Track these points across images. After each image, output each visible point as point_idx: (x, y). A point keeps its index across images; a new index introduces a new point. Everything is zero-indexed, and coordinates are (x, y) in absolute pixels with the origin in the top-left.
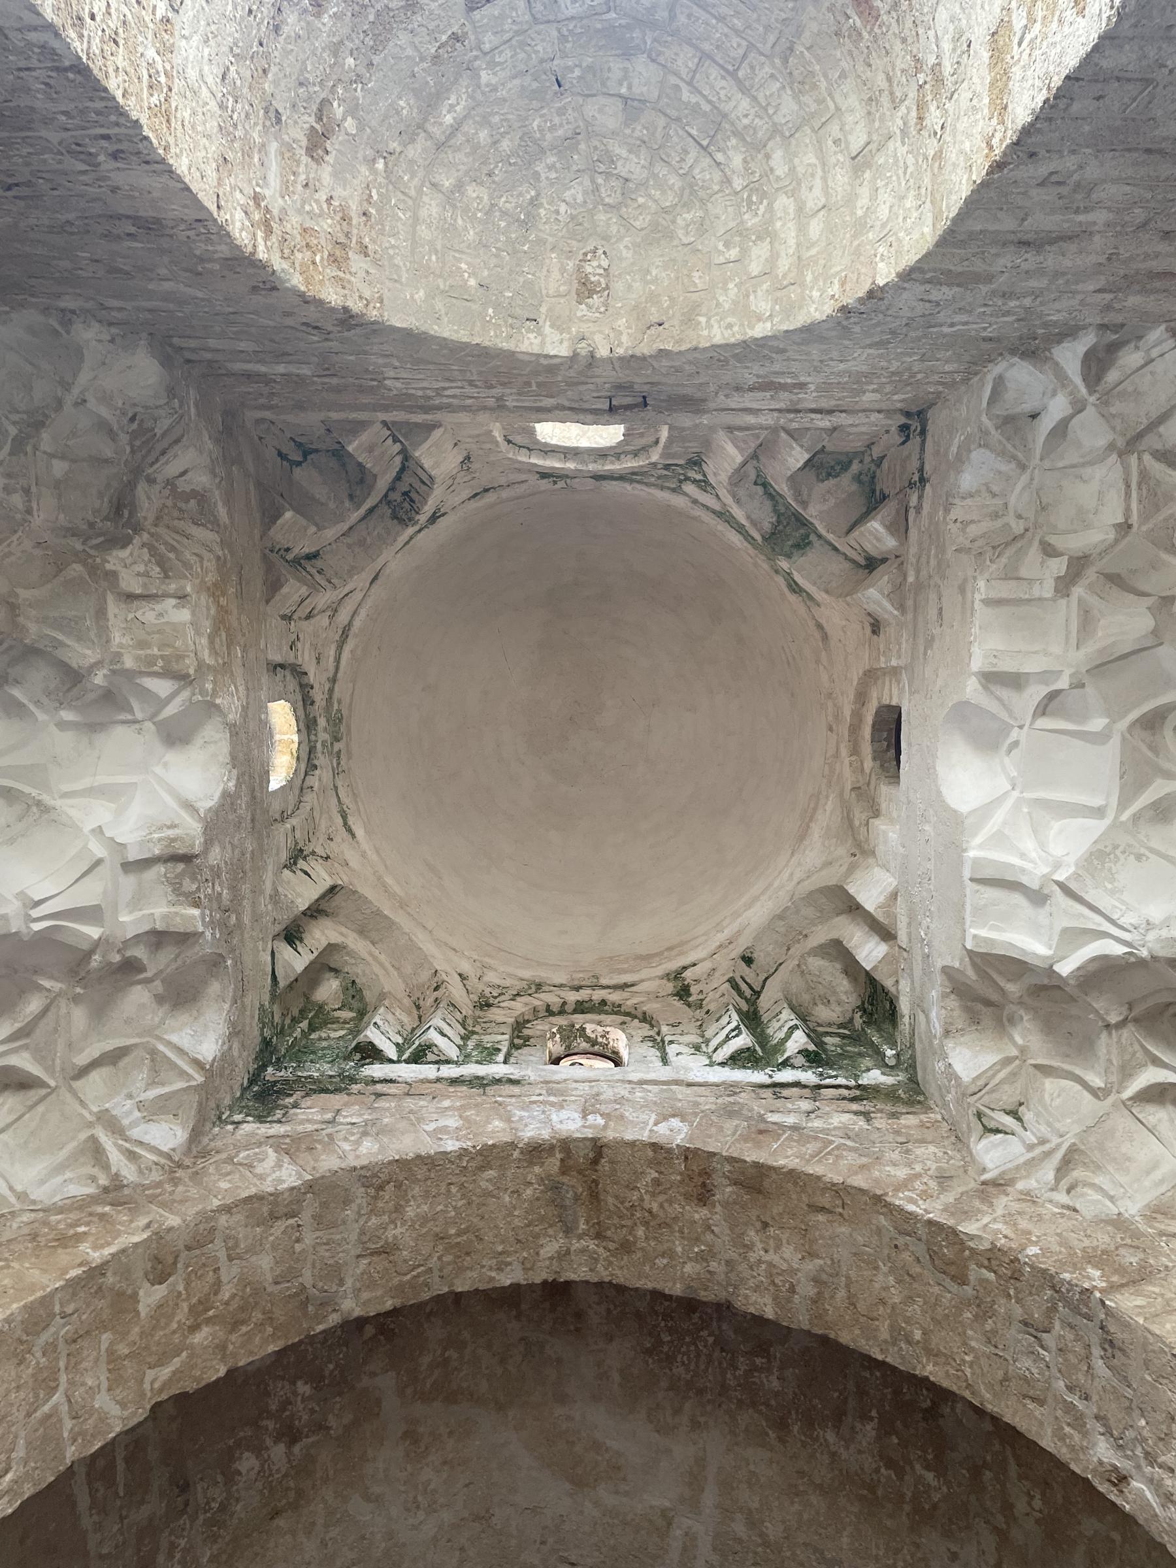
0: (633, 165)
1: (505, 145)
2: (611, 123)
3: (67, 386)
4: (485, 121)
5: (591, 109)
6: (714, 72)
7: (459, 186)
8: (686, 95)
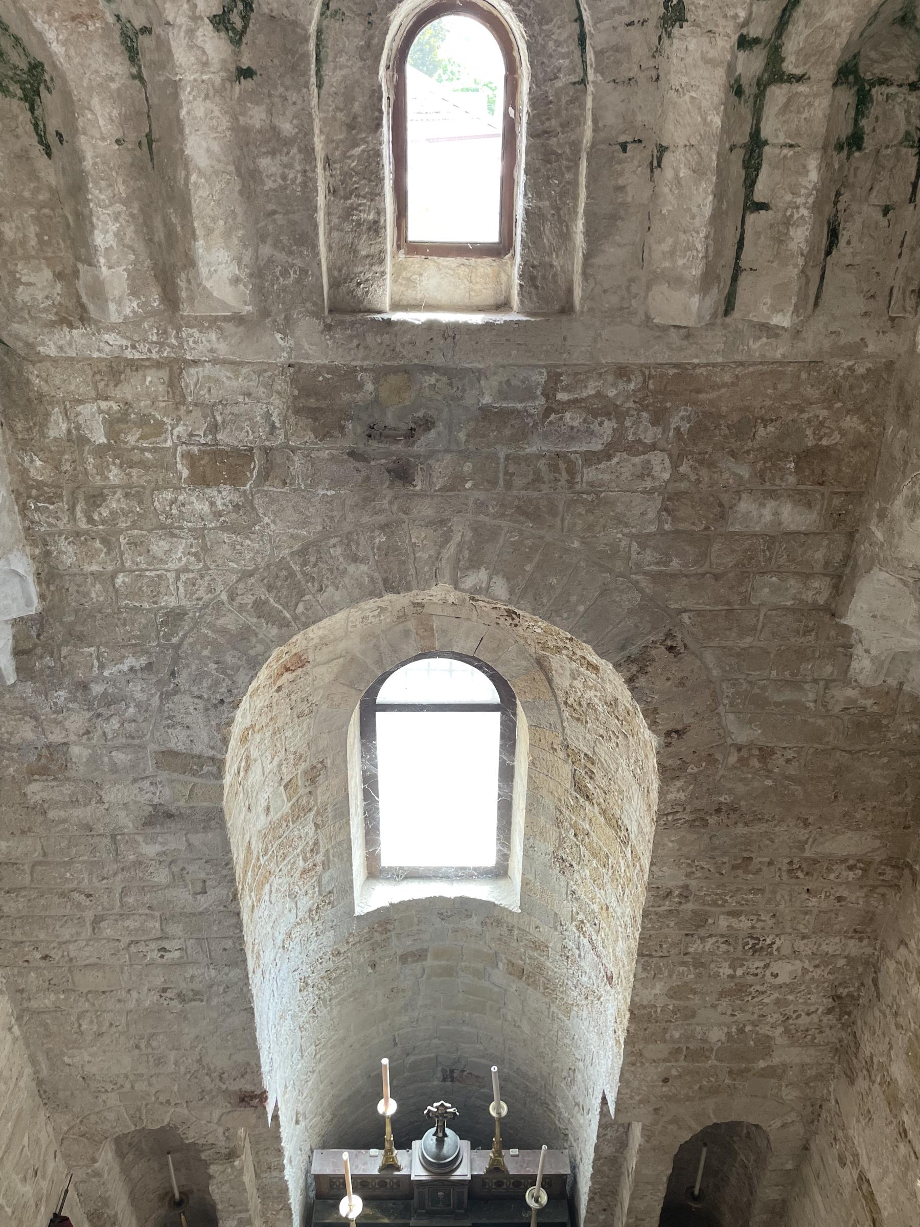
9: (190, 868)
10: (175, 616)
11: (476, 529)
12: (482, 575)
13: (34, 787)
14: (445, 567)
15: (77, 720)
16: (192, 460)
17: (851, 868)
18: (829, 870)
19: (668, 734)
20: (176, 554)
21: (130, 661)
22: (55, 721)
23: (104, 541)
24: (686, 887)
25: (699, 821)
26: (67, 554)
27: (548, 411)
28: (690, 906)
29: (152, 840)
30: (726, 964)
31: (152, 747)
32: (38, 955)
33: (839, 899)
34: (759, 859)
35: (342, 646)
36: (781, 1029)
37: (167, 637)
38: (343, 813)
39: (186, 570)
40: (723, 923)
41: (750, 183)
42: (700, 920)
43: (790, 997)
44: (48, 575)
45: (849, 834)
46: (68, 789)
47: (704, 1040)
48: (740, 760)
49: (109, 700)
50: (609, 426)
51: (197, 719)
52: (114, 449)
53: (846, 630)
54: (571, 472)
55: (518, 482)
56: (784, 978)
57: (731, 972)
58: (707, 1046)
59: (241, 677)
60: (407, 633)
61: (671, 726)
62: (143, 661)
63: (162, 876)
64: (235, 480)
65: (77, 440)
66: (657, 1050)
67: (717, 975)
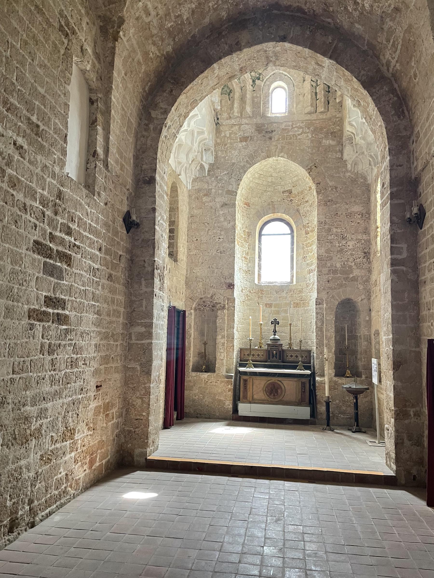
0: (270, 170)
1: (288, 173)
2: (273, 174)
3: (357, 157)
4: (291, 176)
5: (277, 175)
6: (261, 183)
7: (295, 171)
8: (264, 179)
9: (228, 217)
10: (234, 164)
11: (282, 146)
12: (283, 154)
13: (205, 198)
14: (277, 153)
15: (214, 184)
16: (240, 138)
17: (359, 215)
18: (355, 215)
19: (317, 184)
20: (235, 153)
21: (225, 172)
22: (211, 184)
23: (226, 152)
24: (325, 220)
25: (326, 204)
26: (220, 153)
27: (292, 128)
28: (326, 227)
29: (222, 210)
30: (337, 242)
31: (226, 190)
32: (195, 239)
33: (358, 223)
34: (339, 213)
35: (257, 207)
36: (354, 263)
37: (232, 167)
38: (254, 250)
39: (237, 155)
40: (335, 230)
41: (316, 97)
42: (329, 230)
43: (354, 253)
44: (216, 157)
45: (356, 206)
46: (210, 198)
47: (336, 267)
48: (331, 189)
49: (220, 180)
50: (301, 130)
51: (234, 184)
52: (230, 138)
53: (346, 161)
54: (296, 137)
55: (288, 139)
56: (351, 247)
57: (338, 245)
58: (337, 269)
59: (242, 175)
60: (270, 208)
61: (317, 182)
62: (227, 172)
63: (222, 219)
64: (246, 141)
65: (225, 136)
66: (325, 270)
67: (335, 246)
